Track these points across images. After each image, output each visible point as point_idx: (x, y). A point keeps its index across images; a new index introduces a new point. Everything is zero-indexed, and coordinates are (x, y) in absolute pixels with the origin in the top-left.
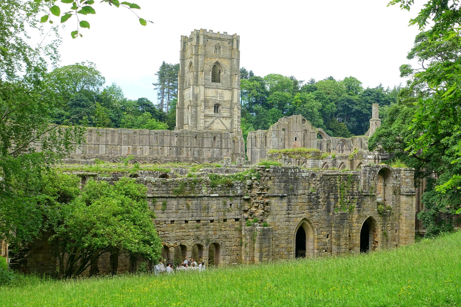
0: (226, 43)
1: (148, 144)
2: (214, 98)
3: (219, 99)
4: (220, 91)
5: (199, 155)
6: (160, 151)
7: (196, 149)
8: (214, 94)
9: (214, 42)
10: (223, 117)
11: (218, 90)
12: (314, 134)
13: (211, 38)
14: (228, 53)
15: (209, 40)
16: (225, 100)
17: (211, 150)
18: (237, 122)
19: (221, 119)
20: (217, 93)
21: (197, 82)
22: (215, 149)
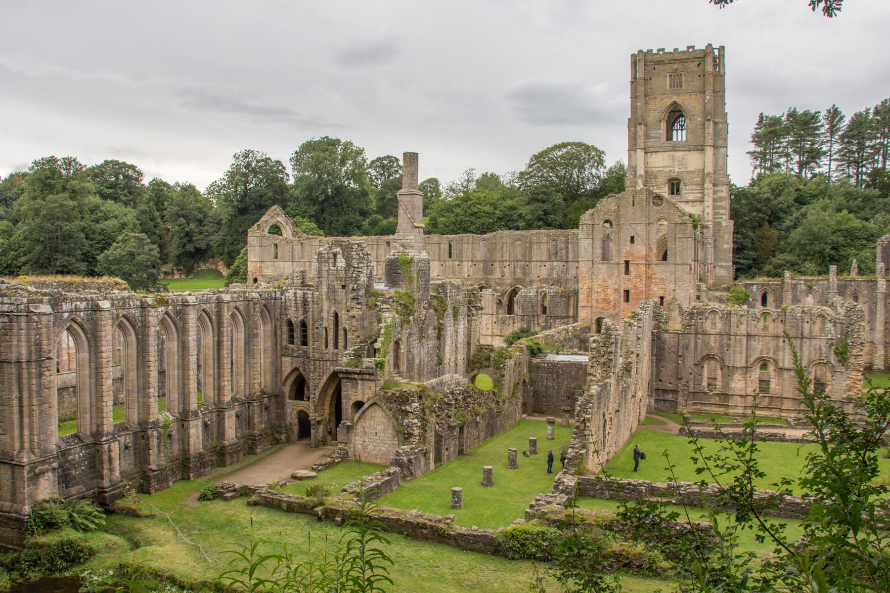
0: (693, 66)
1: (436, 258)
2: (668, 169)
3: (677, 169)
4: (679, 155)
5: (524, 274)
6: (457, 268)
7: (520, 263)
8: (667, 162)
9: (669, 68)
10: (687, 202)
12: (682, 227)
13: (659, 62)
14: (697, 83)
15: (656, 67)
16: (691, 168)
17: (548, 264)
20: (673, 159)
21: (635, 145)
22: (555, 264)
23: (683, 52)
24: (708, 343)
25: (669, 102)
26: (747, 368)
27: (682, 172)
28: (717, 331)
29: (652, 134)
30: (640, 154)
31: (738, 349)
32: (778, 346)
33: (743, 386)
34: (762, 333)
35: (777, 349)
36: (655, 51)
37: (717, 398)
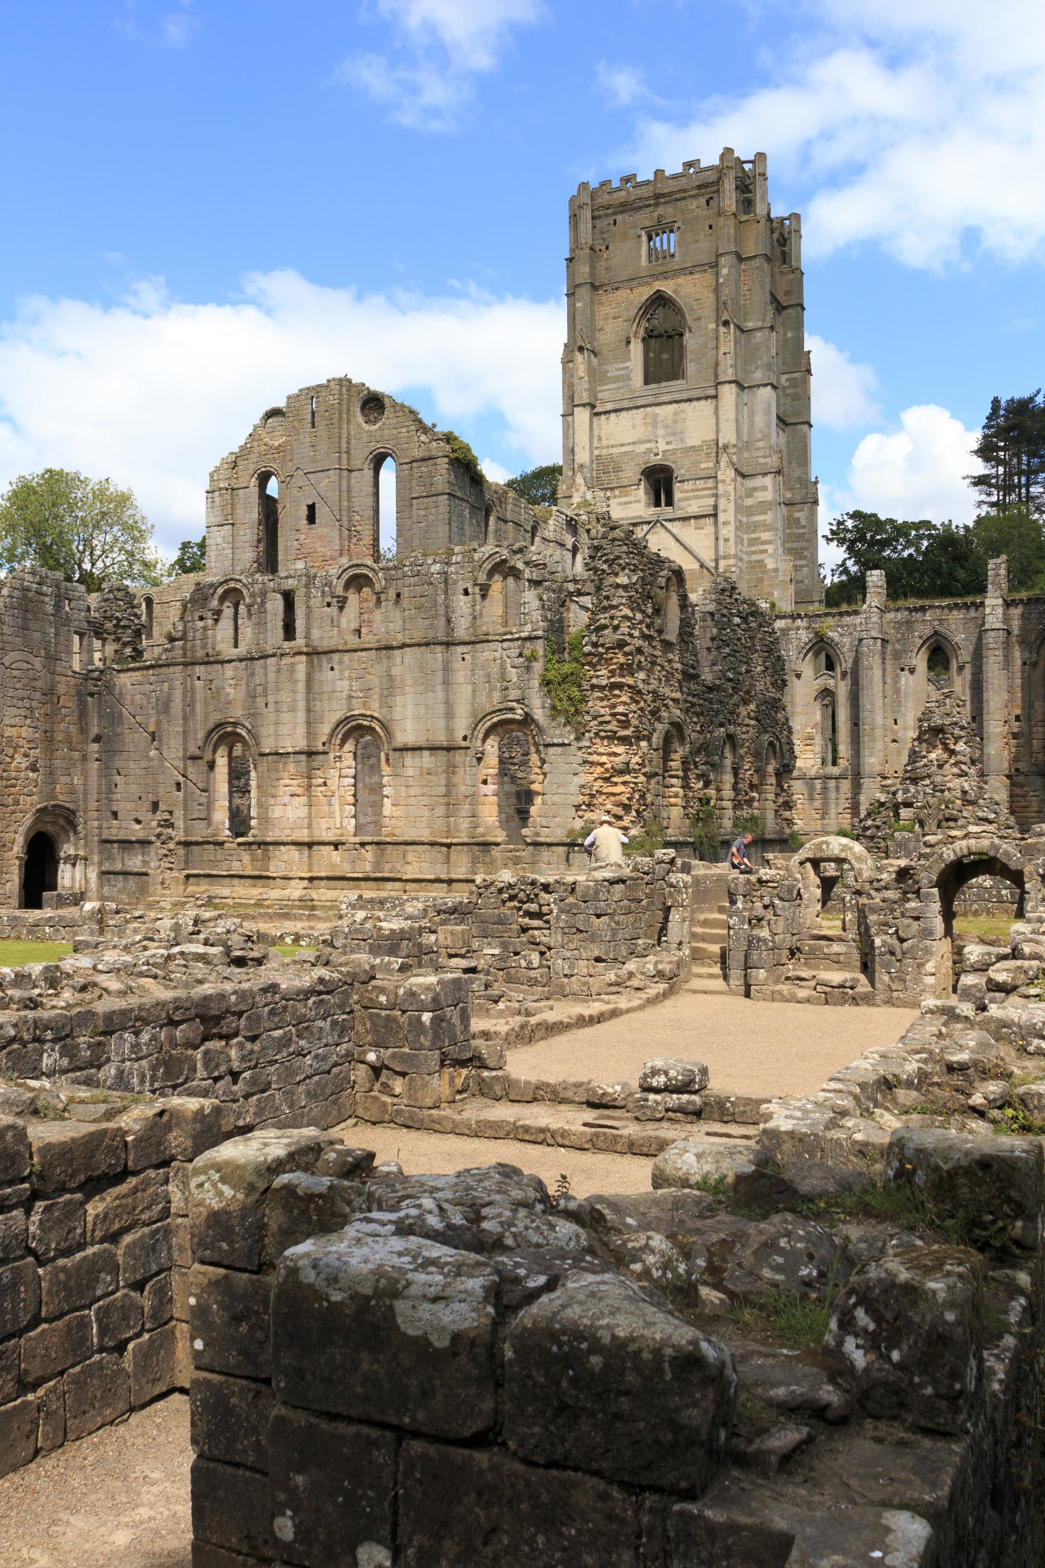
2: (642, 448)
3: (662, 446)
4: (665, 412)
8: (640, 433)
9: (645, 218)
10: (685, 519)
11: (657, 410)
13: (625, 207)
16: (693, 441)
18: (732, 527)
19: (675, 527)
20: (654, 424)
23: (675, 177)
24: (219, 689)
25: (645, 293)
26: (310, 754)
27: (674, 452)
28: (242, 650)
29: (612, 370)
30: (582, 415)
31: (285, 697)
32: (390, 677)
33: (303, 812)
34: (353, 641)
35: (390, 687)
36: (616, 184)
37: (246, 857)
